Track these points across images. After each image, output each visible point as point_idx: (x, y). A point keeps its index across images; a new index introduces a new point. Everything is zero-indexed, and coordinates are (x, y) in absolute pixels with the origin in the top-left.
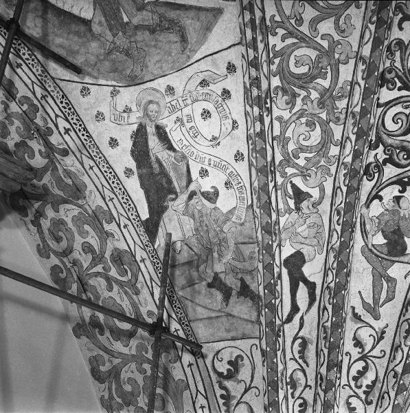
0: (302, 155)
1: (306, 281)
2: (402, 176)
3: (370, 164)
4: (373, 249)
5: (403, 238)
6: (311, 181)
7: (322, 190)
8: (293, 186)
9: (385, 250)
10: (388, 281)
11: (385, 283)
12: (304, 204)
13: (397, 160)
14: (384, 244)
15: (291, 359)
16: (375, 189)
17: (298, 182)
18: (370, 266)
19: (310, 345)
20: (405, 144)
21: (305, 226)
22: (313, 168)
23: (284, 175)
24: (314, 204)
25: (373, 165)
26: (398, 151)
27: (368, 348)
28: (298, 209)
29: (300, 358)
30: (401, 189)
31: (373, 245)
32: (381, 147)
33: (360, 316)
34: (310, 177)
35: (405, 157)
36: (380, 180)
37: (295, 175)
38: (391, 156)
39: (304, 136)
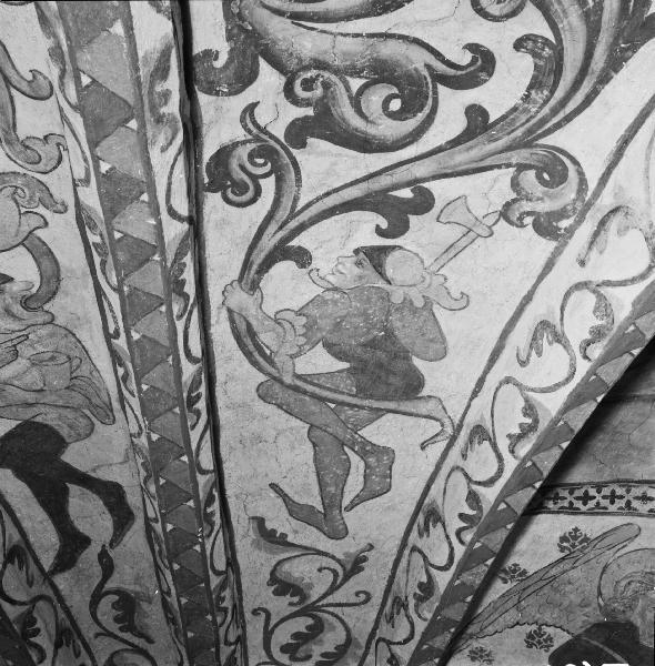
2: (385, 181)
3: (224, 154)
4: (299, 383)
5: (407, 359)
7: (43, 255)
9: (348, 384)
10: (363, 454)
11: (355, 459)
13: (356, 122)
14: (348, 369)
15: (97, 635)
16: (272, 227)
18: (295, 423)
19: (145, 606)
20: (389, 50)
25: (243, 153)
26: (356, 84)
27: (314, 595)
29: (121, 629)
30: (384, 225)
31: (299, 377)
32: (269, 79)
35: (396, 105)
36: (287, 203)
38: (324, 109)
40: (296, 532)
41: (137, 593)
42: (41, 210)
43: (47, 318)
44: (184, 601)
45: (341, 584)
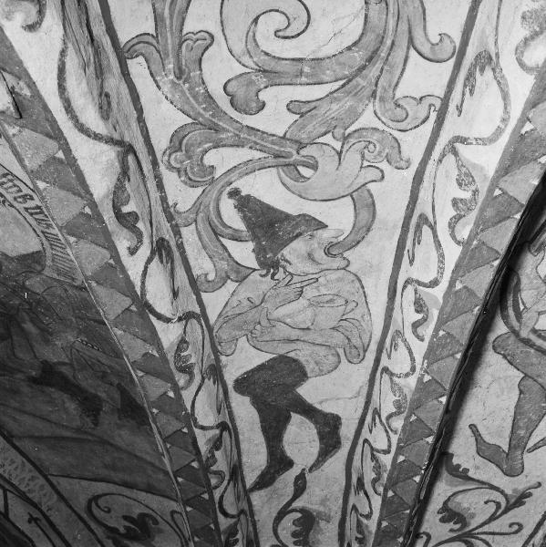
0: (276, 96)
1: (309, 411)
4: (533, 337)
6: (327, 175)
7: (365, 205)
8: (245, 204)
12: (294, 252)
17: (268, 188)
19: (322, 524)
21: (303, 302)
22: (328, 139)
23: (199, 175)
24: (332, 245)
27: (474, 524)
28: (270, 265)
31: (534, 331)
33: (466, 470)
34: (315, 167)
37: (248, 168)
39: (277, 21)
40: (477, 468)
41: (319, 513)
42: (384, 165)
43: (343, 263)
44: (385, 524)
45: (500, 516)
